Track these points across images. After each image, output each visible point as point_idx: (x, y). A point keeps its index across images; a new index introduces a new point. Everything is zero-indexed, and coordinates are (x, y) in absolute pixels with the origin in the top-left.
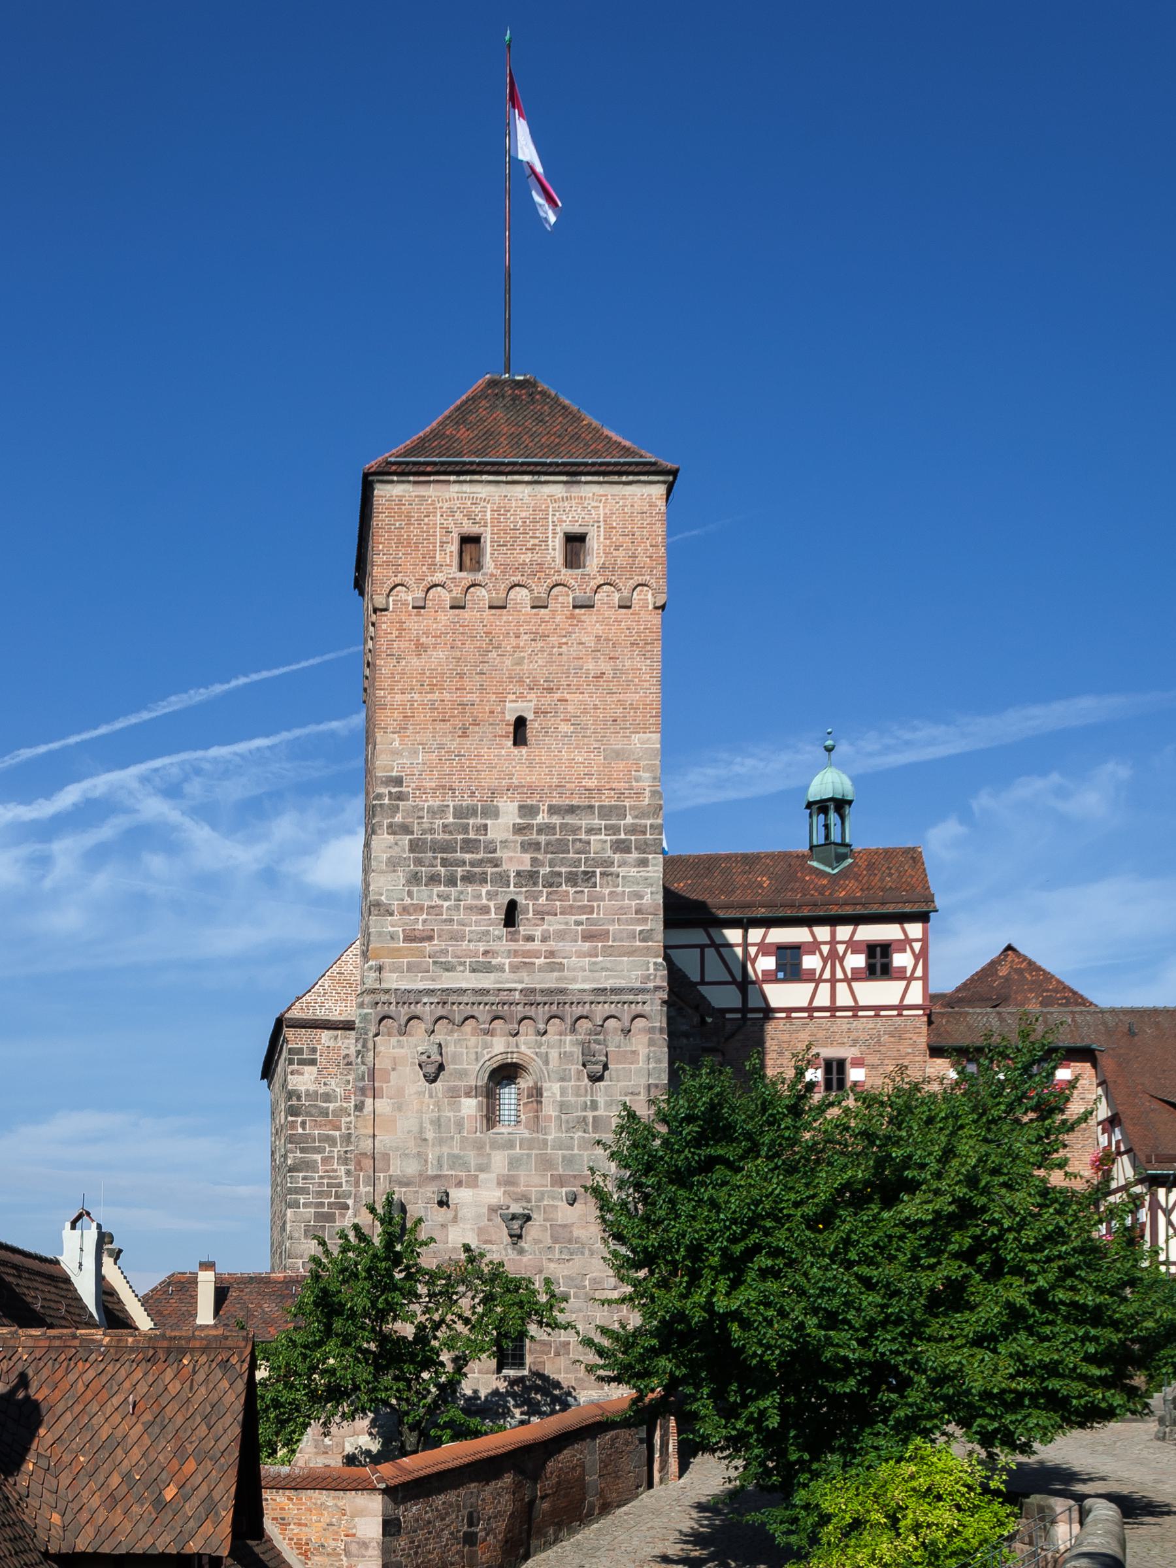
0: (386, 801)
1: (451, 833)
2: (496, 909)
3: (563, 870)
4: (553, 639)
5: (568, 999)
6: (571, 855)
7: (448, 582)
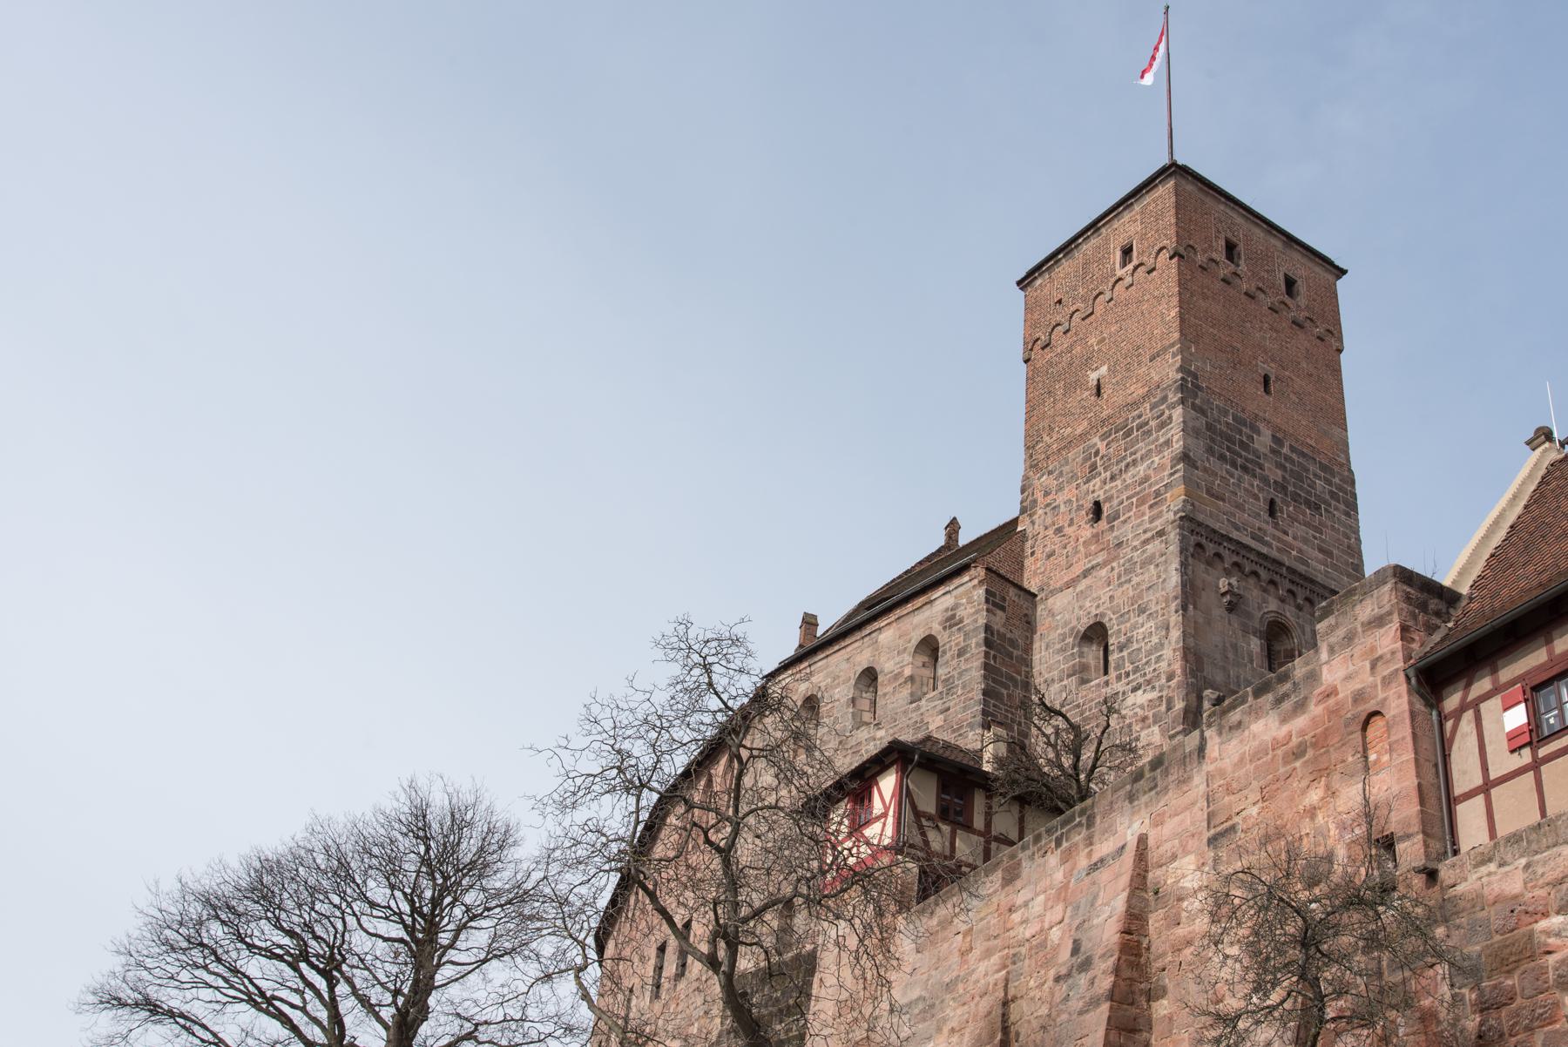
5: (1316, 589)
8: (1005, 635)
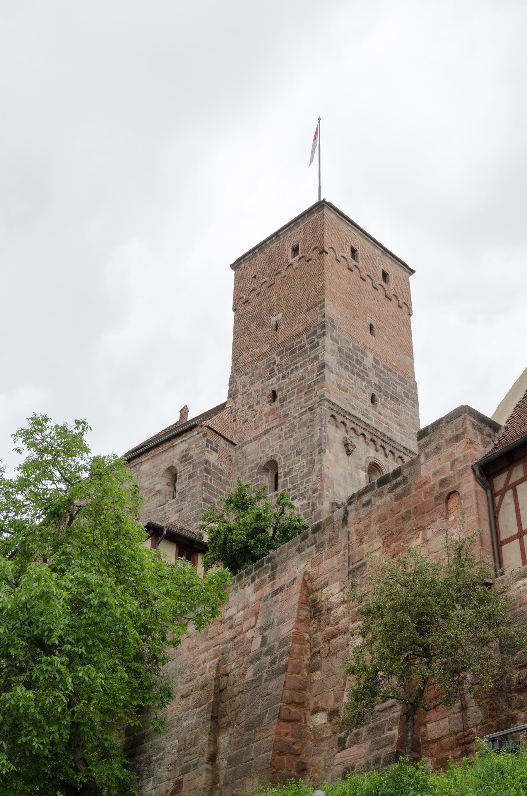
8: (217, 467)
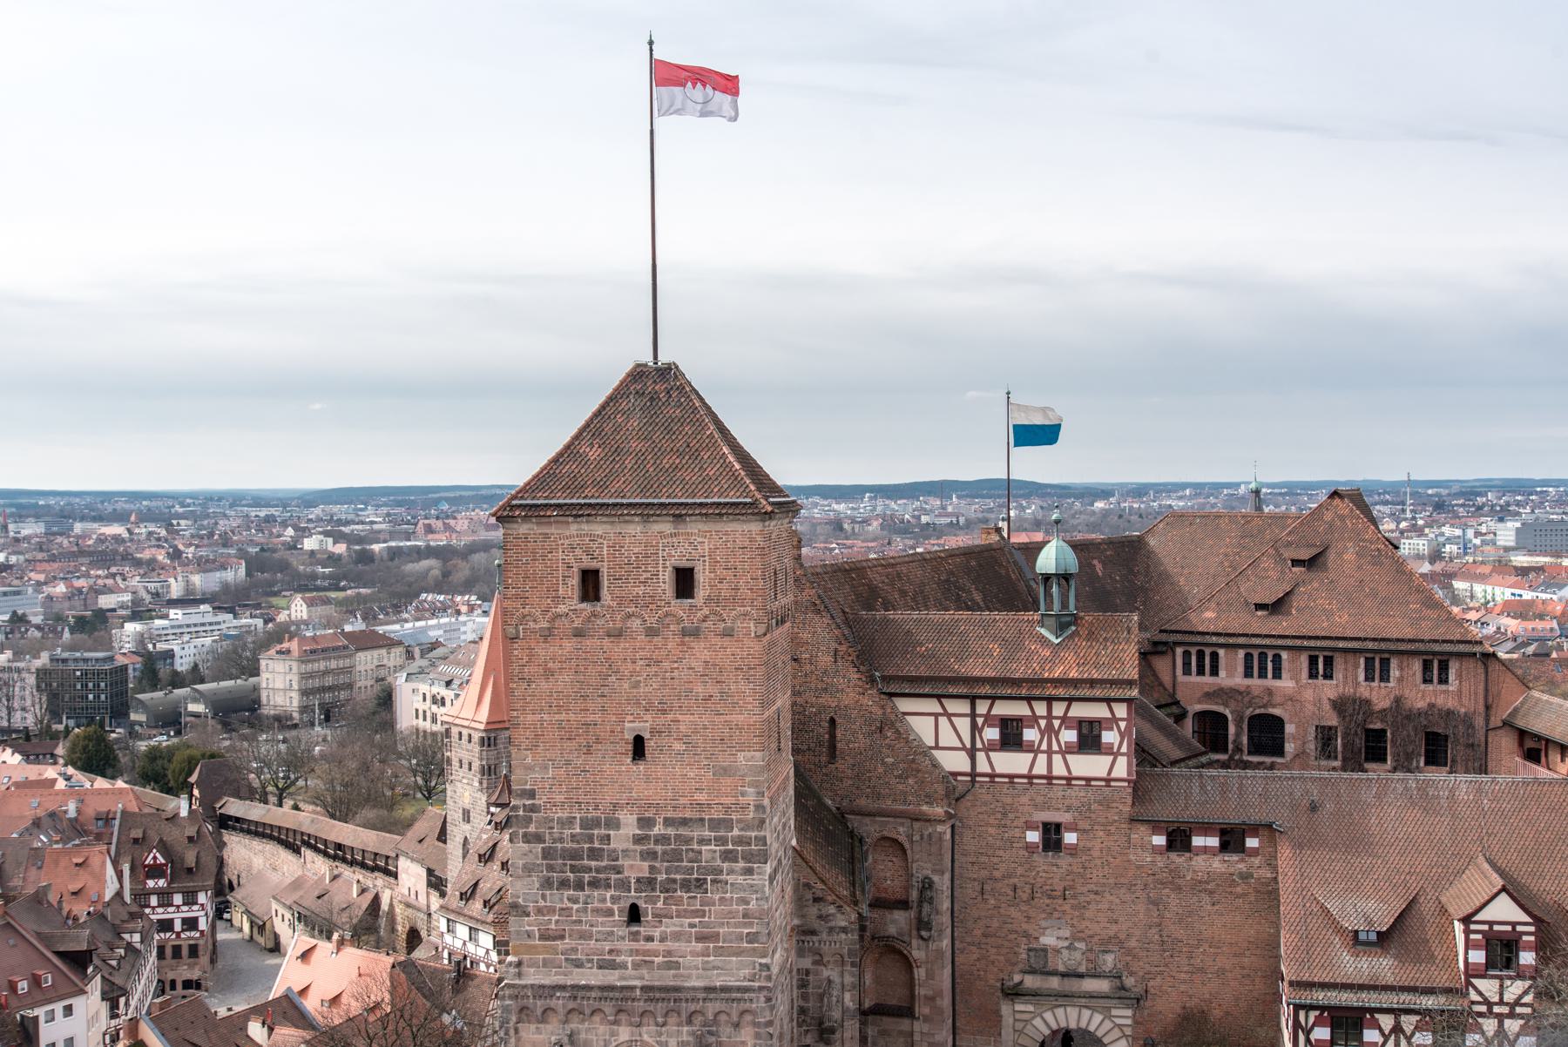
0: (521, 813)
1: (578, 842)
2: (619, 911)
3: (678, 877)
4: (666, 664)
6: (685, 864)
7: (571, 613)
